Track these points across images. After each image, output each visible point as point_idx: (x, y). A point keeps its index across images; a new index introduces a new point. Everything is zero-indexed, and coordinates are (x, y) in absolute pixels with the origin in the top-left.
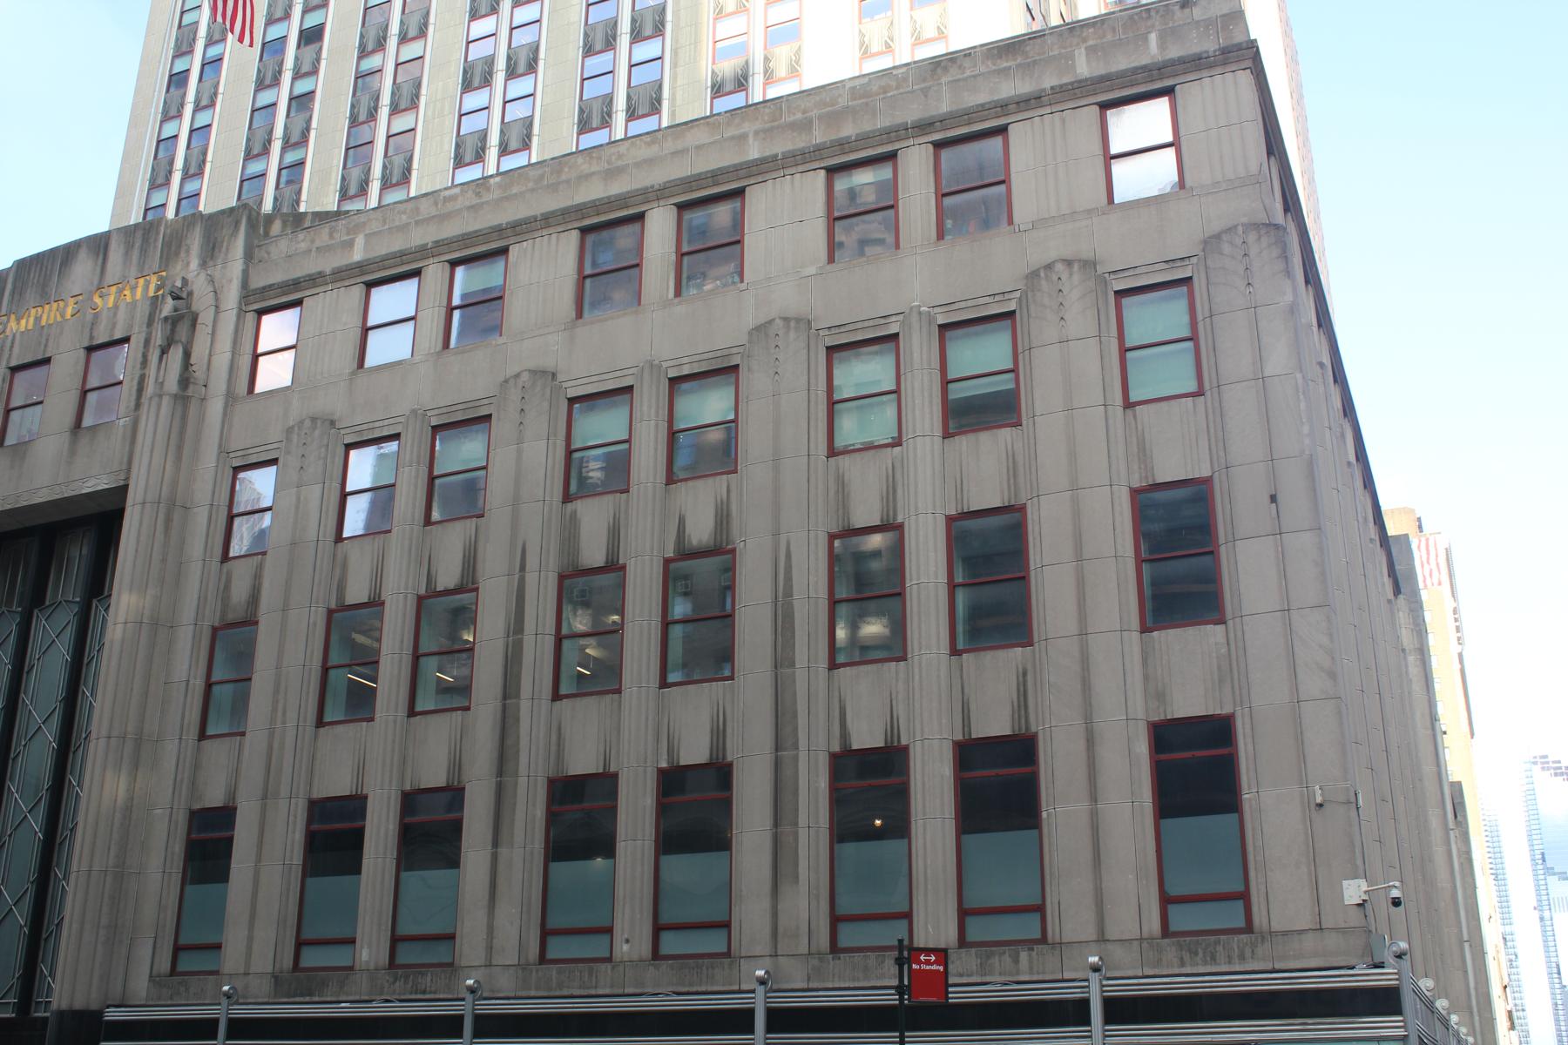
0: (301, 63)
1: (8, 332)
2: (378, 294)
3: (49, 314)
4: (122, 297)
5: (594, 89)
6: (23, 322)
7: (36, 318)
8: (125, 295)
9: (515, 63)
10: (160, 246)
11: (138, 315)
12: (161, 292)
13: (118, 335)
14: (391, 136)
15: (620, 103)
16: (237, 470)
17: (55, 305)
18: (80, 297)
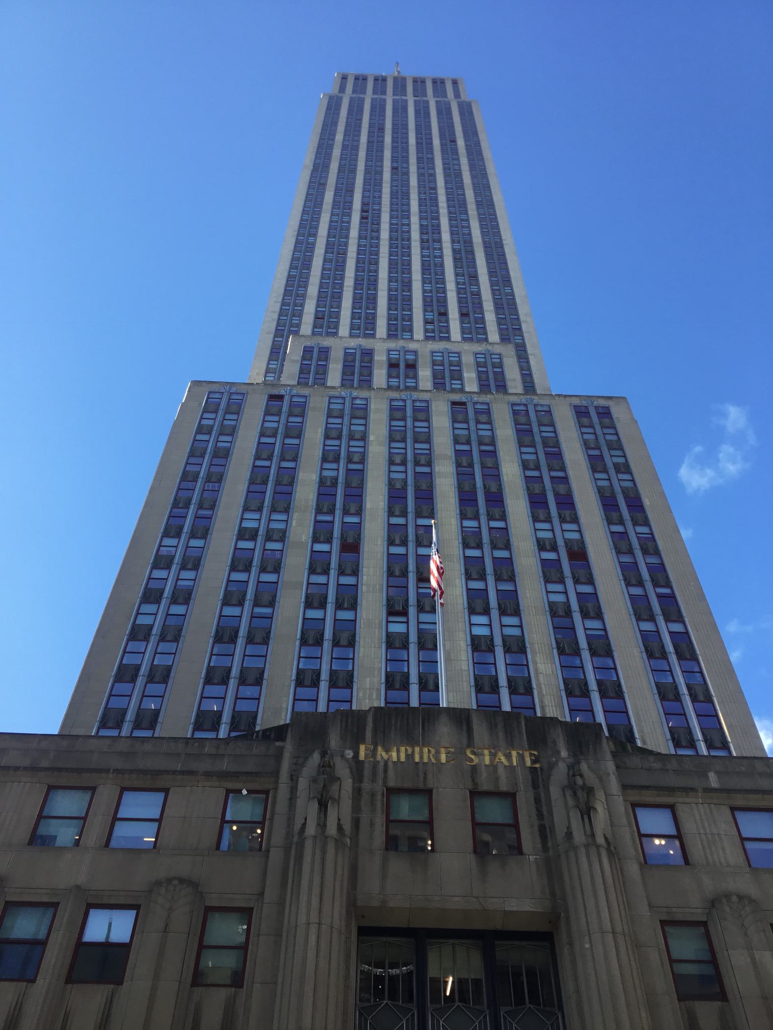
0: (254, 635)
1: (379, 758)
2: (128, 797)
3: (422, 754)
4: (497, 760)
5: (116, 703)
6: (394, 754)
7: (407, 756)
8: (500, 759)
9: (426, 683)
10: (524, 732)
11: (521, 777)
12: (537, 766)
13: (504, 787)
14: (204, 698)
15: (130, 716)
16: (91, 906)
17: (426, 750)
18: (452, 750)
